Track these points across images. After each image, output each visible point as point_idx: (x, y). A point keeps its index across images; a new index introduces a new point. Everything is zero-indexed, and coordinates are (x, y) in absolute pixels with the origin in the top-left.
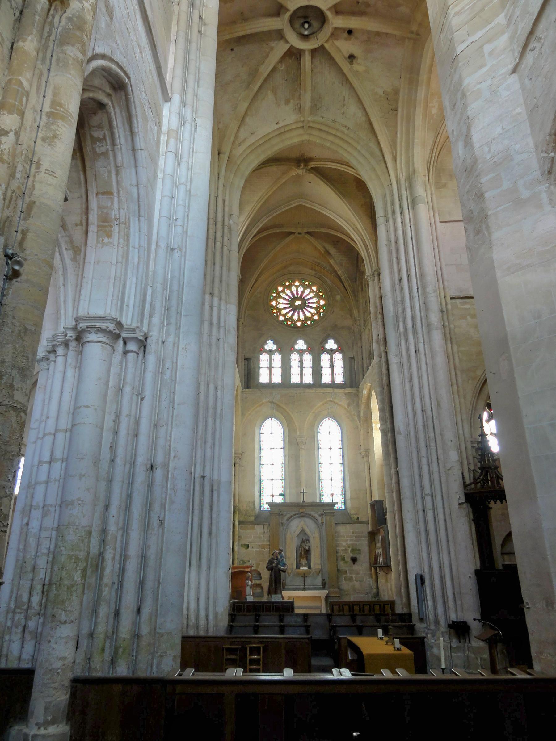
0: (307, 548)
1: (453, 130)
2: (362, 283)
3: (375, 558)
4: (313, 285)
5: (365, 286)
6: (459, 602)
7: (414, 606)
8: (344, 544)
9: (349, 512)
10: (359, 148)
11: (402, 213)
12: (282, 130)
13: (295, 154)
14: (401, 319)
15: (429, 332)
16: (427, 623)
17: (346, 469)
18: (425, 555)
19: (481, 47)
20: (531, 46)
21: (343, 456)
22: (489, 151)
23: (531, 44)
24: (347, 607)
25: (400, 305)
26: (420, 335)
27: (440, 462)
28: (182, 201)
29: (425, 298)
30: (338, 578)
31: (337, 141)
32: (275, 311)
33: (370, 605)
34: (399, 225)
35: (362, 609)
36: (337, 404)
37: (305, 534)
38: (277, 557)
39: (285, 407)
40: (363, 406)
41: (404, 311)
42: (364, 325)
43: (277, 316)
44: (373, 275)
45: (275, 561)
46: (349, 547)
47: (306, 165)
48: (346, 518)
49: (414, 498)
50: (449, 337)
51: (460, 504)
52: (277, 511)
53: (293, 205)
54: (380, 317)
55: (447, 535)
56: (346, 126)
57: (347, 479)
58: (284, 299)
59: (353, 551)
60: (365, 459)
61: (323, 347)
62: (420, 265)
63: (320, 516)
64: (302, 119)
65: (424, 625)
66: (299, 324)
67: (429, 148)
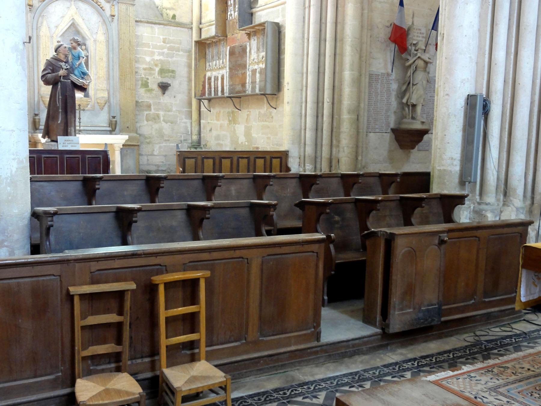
8: (148, 59)
18: (500, 55)
37: (78, 32)
45: (63, 64)
46: (156, 65)
59: (162, 71)
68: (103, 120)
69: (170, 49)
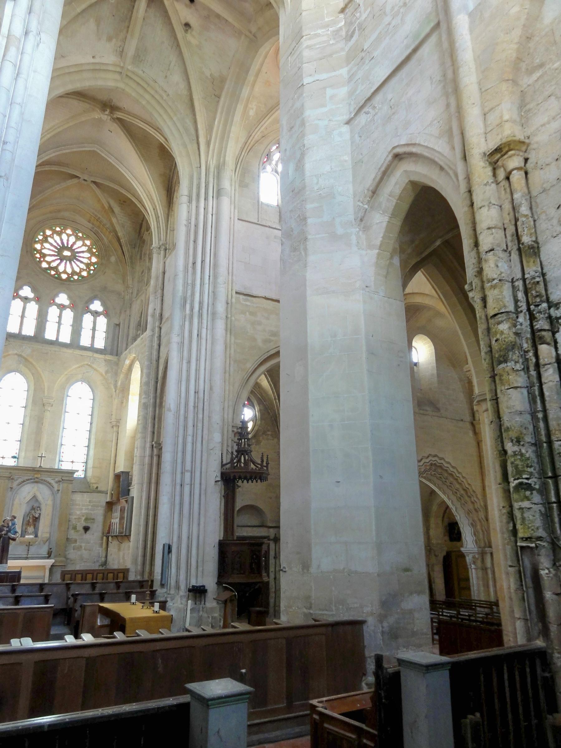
0: (37, 516)
1: (286, 150)
2: (141, 251)
3: (109, 528)
4: (88, 238)
5: (145, 254)
6: (200, 569)
7: (158, 573)
9: (88, 480)
10: (175, 119)
11: (206, 199)
12: (97, 67)
13: (104, 97)
14: (188, 301)
15: (213, 320)
16: (167, 589)
17: (93, 437)
18: (176, 526)
19: (325, 88)
20: (366, 109)
21: (91, 424)
22: (317, 183)
23: (366, 107)
24: (112, 575)
25: (190, 287)
26: (205, 322)
27: (204, 441)
28: (16, 123)
29: (215, 287)
30: (66, 547)
31: (153, 102)
32: (38, 255)
33: (82, 574)
34: (202, 210)
35: (84, 578)
36: (95, 370)
37: (37, 500)
38: (8, 524)
39: (34, 363)
40: (122, 376)
41: (193, 294)
42: (137, 294)
43: (40, 262)
44: (159, 248)
46: (83, 516)
47: (111, 113)
48: (85, 486)
49: (174, 473)
50: (230, 329)
51: (216, 482)
52: (7, 475)
53: (87, 149)
54: (160, 291)
55: (200, 509)
56: (166, 92)
57: (92, 446)
58: (51, 245)
59: (86, 519)
60: (115, 429)
61: (88, 307)
62: (215, 255)
63: (57, 482)
64: (122, 65)
65: (164, 590)
66: (64, 276)
67: (240, 145)
68: (44, 551)
69: (92, 506)
